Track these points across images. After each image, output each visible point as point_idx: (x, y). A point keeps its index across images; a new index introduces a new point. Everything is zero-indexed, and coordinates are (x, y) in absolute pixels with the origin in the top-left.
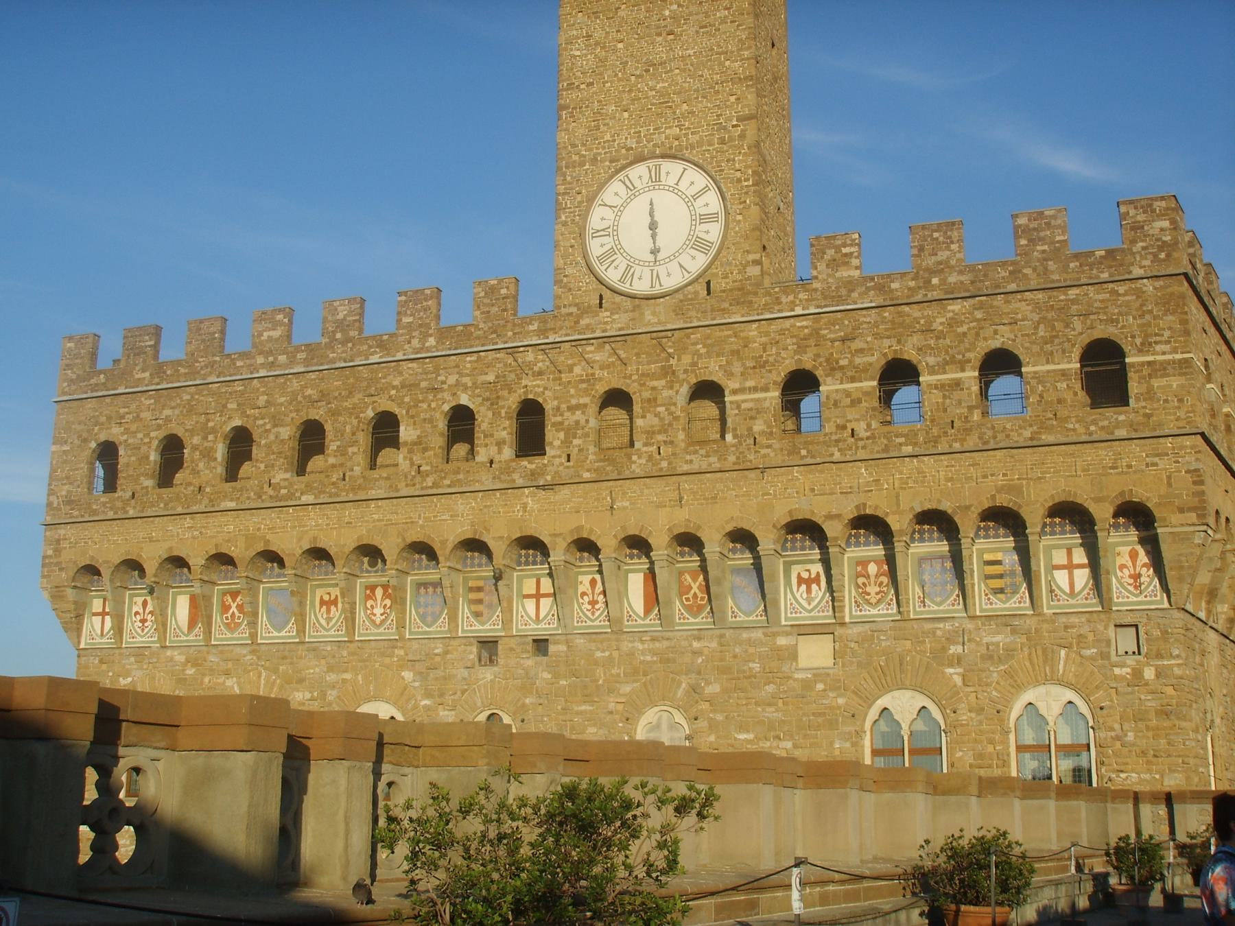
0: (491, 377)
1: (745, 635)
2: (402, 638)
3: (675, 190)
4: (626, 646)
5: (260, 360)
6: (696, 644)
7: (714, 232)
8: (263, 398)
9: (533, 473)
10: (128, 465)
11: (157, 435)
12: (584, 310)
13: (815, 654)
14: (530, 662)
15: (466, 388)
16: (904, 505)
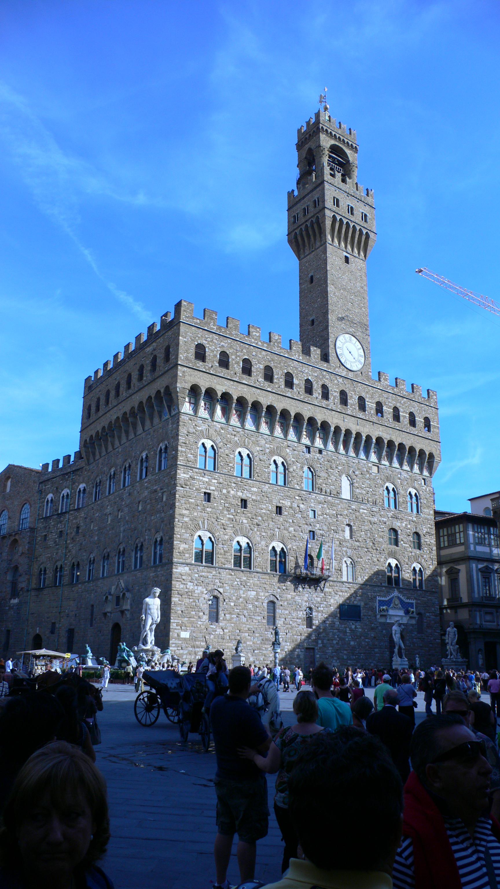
0: (316, 375)
1: (363, 461)
2: (286, 439)
3: (354, 345)
4: (340, 457)
5: (253, 340)
6: (354, 461)
7: (363, 360)
8: (254, 353)
9: (328, 405)
10: (209, 355)
11: (220, 350)
12: (337, 367)
13: (375, 469)
14: (318, 455)
15: (310, 375)
16: (398, 440)
